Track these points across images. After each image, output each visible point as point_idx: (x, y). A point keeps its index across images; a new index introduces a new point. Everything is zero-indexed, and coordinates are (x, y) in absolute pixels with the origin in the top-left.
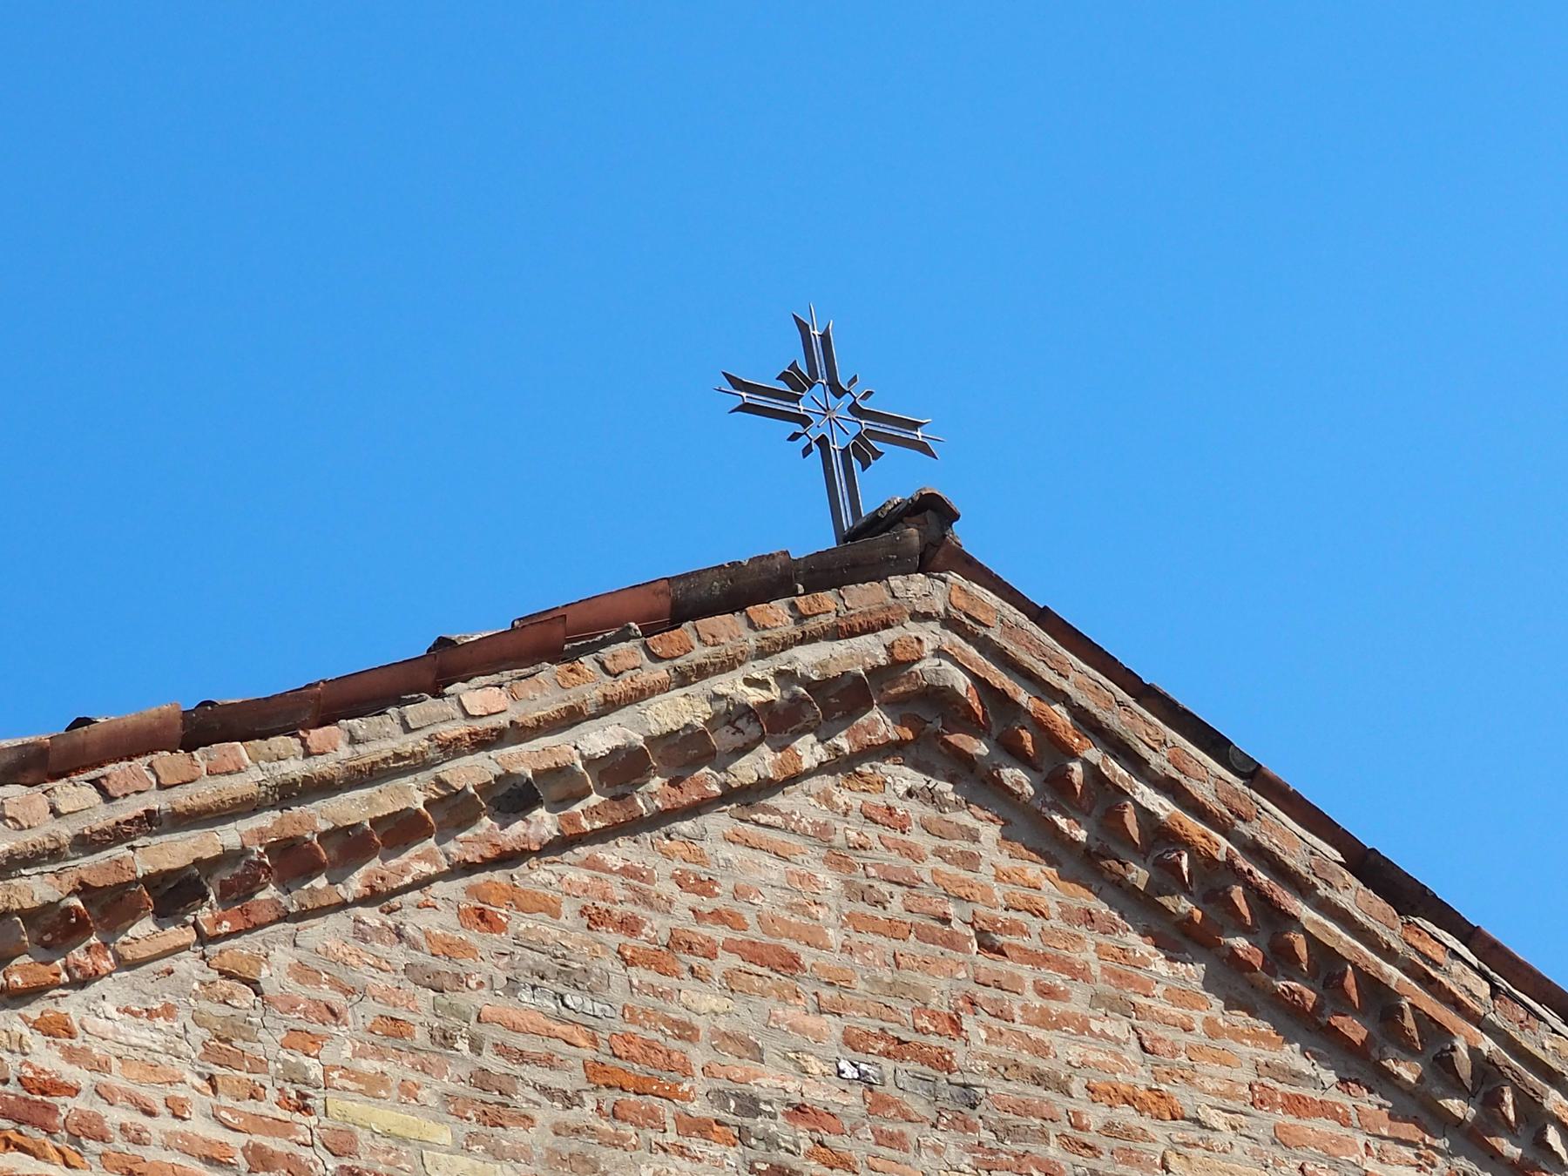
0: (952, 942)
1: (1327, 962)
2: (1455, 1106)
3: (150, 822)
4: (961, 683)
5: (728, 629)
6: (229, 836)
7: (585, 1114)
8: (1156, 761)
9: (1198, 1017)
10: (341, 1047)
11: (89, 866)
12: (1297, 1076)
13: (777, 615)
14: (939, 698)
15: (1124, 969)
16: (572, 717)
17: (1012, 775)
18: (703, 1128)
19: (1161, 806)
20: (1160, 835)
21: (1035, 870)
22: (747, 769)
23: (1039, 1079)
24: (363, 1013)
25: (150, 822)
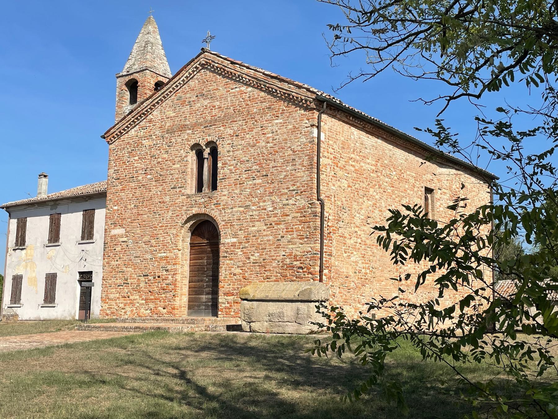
0: (205, 82)
1: (228, 72)
2: (238, 79)
3: (154, 100)
4: (204, 62)
5: (190, 66)
6: (160, 98)
7: (180, 107)
8: (216, 62)
9: (221, 81)
10: (167, 109)
11: (152, 104)
12: (227, 82)
13: (193, 63)
14: (203, 64)
15: (216, 79)
16: (180, 79)
17: (209, 67)
18: (186, 105)
19: (216, 65)
20: (217, 67)
21: (211, 74)
22: (191, 76)
23: (209, 91)
24: (168, 106)
25: (154, 100)
